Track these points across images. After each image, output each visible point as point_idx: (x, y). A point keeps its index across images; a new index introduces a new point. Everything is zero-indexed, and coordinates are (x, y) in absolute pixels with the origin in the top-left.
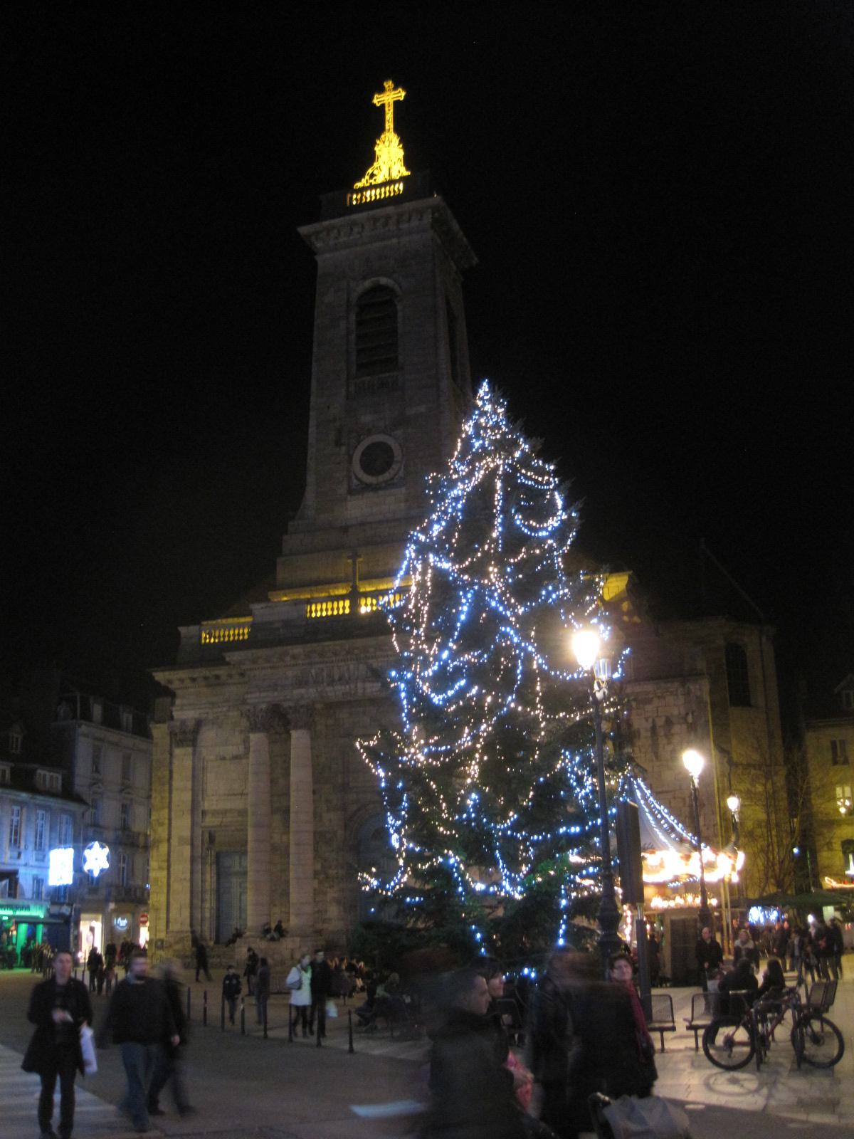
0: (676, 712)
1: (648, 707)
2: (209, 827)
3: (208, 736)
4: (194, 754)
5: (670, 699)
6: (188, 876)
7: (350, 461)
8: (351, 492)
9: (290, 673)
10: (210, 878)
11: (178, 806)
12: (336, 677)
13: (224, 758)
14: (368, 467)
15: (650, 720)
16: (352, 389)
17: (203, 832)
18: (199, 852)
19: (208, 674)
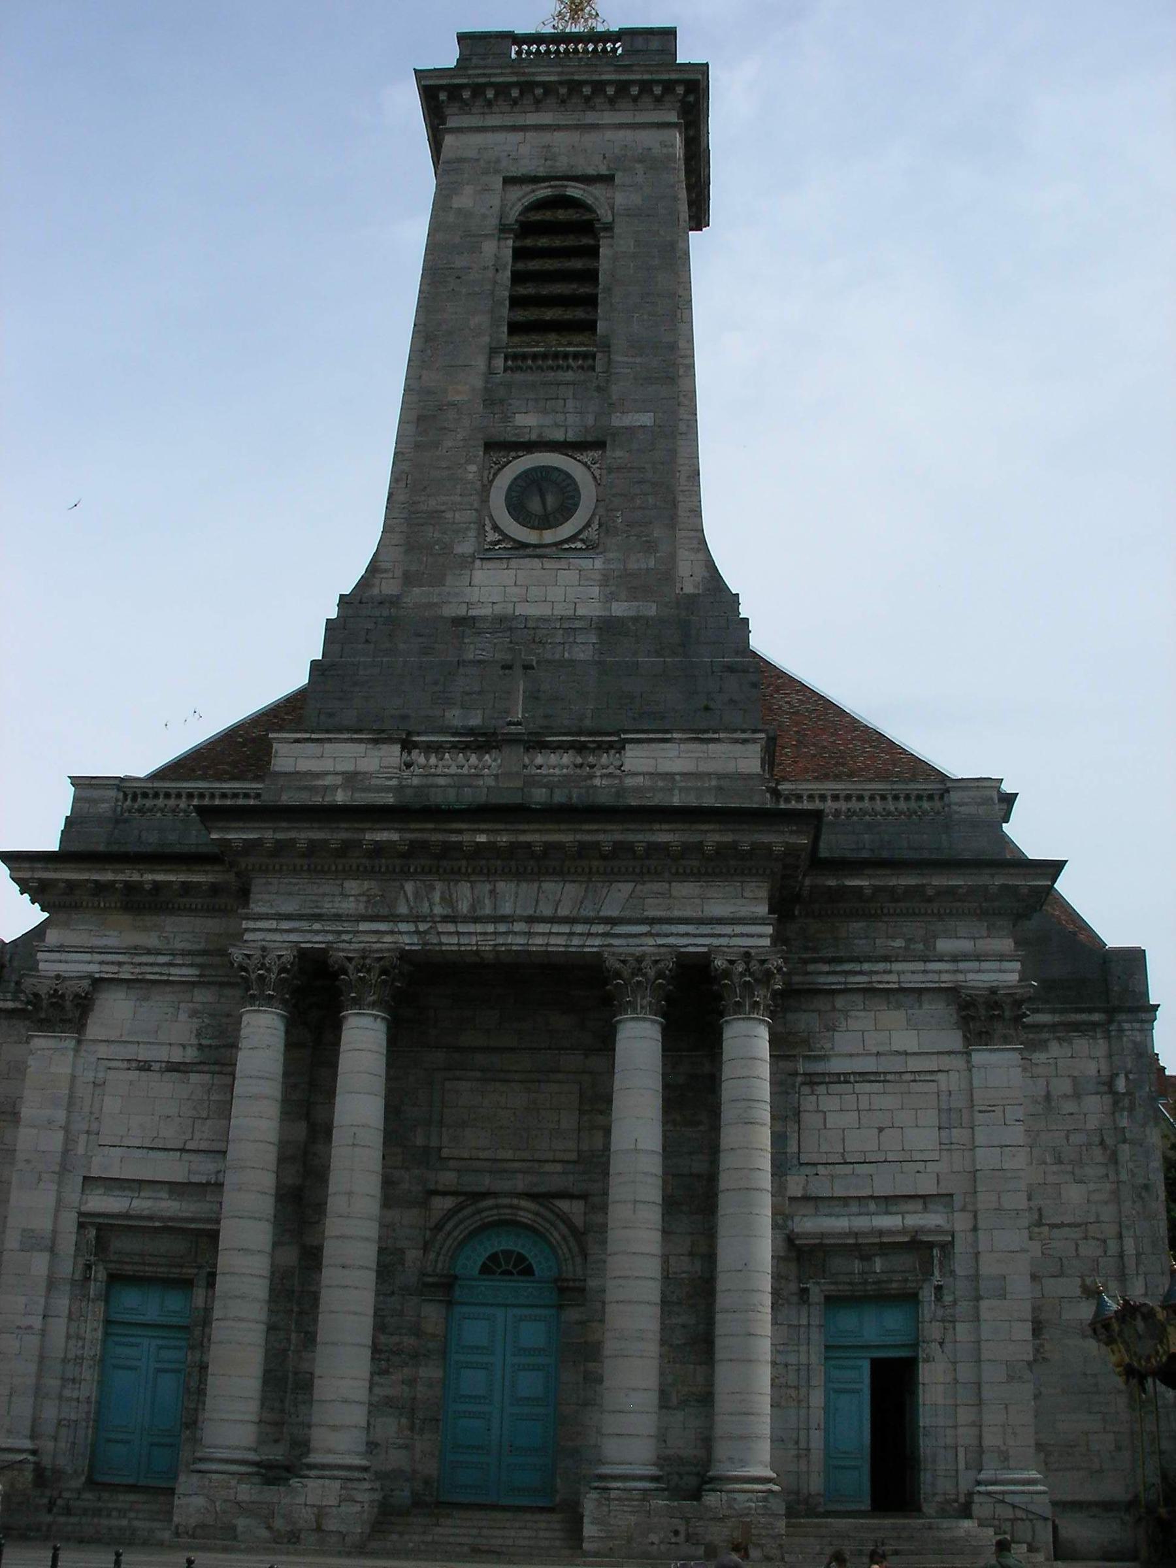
0: (1091, 1069)
1: (1039, 1057)
2: (99, 1215)
3: (115, 1013)
4: (76, 1051)
5: (1081, 1044)
6: (37, 1322)
7: (485, 500)
8: (487, 554)
9: (352, 886)
10: (93, 1330)
11: (28, 1161)
12: (464, 908)
13: (145, 1067)
14: (517, 508)
15: (1042, 1082)
16: (499, 362)
17: (81, 1226)
18: (66, 1268)
19: (136, 877)
